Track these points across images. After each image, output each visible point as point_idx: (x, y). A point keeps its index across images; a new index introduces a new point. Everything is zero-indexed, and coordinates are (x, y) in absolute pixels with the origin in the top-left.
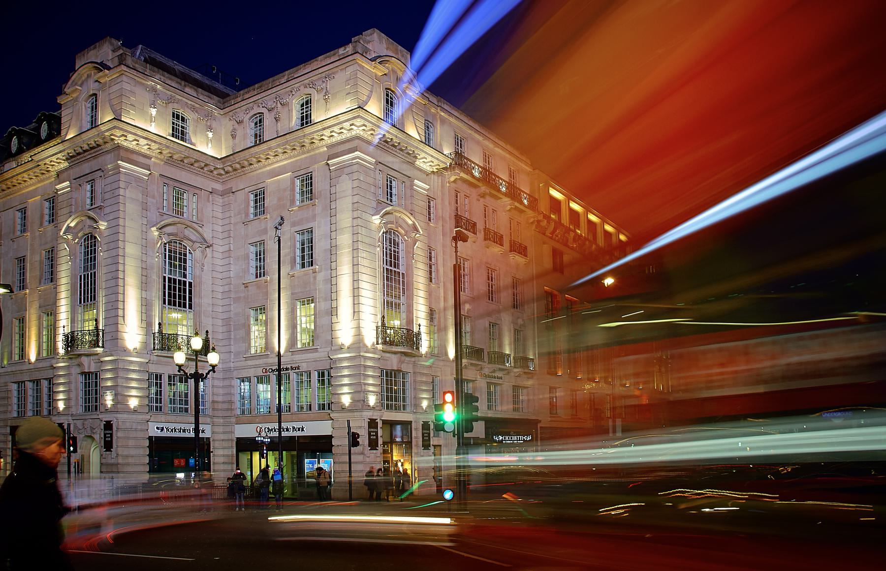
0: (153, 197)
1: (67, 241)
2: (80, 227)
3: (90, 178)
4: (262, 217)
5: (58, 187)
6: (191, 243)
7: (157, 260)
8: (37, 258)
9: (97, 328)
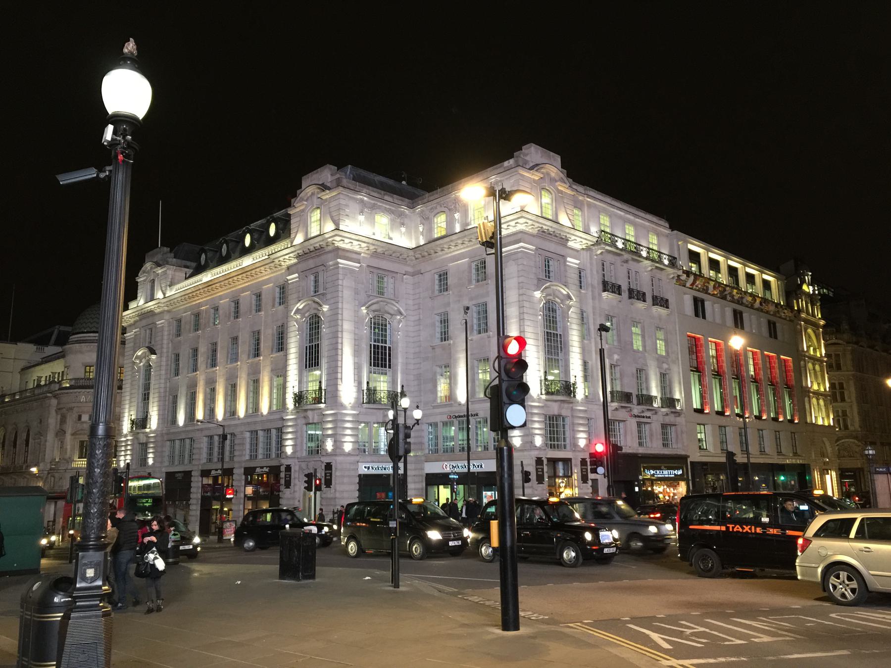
0: (363, 283)
1: (296, 321)
2: (307, 308)
3: (314, 271)
4: (446, 293)
5: (289, 278)
6: (389, 316)
7: (366, 331)
8: (270, 331)
9: (320, 388)
